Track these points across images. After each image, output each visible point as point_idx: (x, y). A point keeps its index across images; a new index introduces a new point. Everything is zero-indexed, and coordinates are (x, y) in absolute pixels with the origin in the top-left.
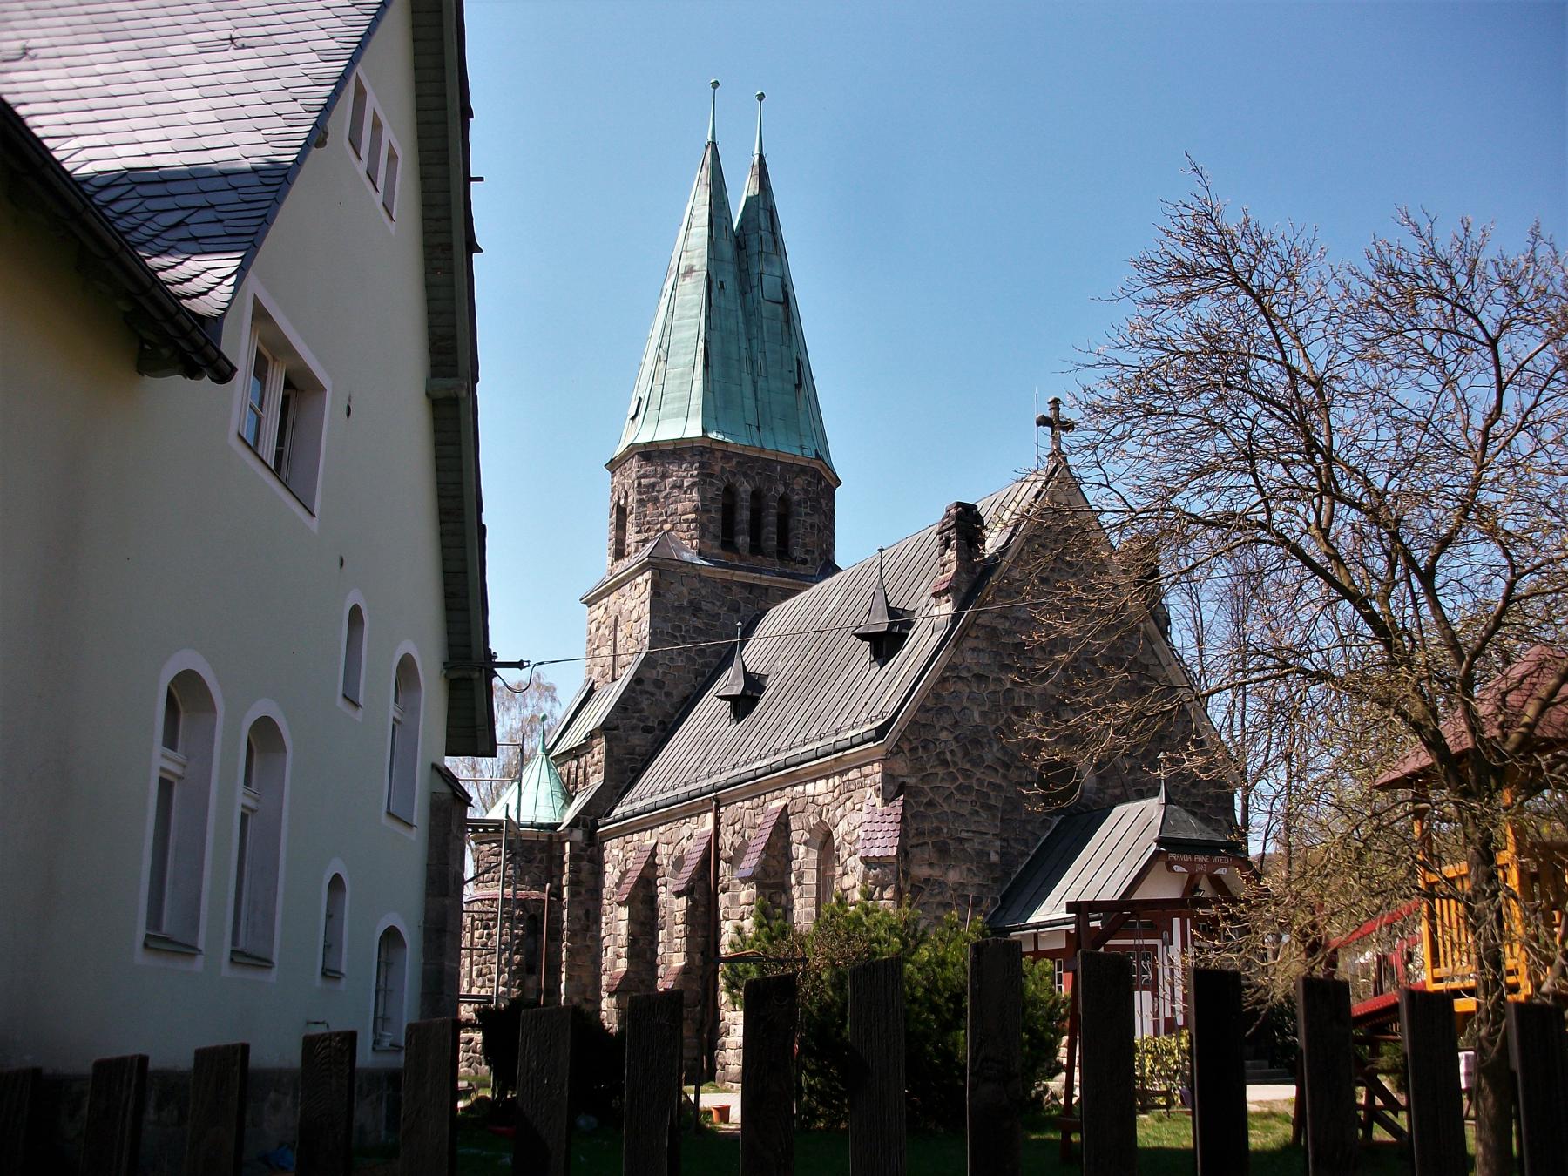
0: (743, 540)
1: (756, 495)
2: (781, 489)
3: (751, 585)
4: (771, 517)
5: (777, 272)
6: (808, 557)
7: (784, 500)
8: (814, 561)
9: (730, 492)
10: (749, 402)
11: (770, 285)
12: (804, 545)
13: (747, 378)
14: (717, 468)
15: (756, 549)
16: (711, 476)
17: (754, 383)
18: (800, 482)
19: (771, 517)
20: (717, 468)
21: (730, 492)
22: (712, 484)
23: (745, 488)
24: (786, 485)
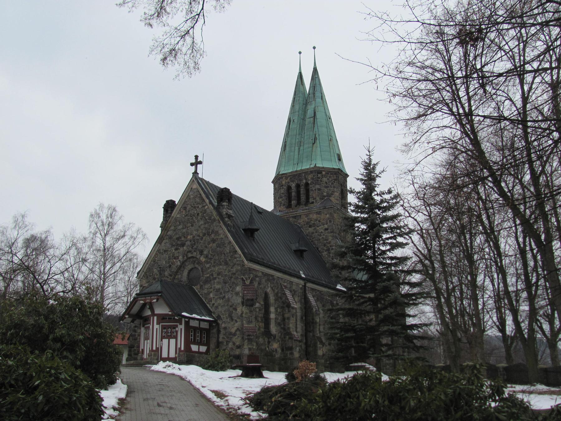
0: (294, 202)
1: (298, 186)
2: (304, 181)
3: (295, 216)
4: (302, 190)
5: (313, 106)
6: (314, 201)
7: (307, 184)
8: (316, 202)
9: (289, 188)
10: (296, 156)
11: (310, 113)
12: (313, 197)
13: (297, 148)
14: (284, 182)
15: (299, 203)
16: (282, 186)
17: (299, 149)
18: (310, 177)
19: (302, 190)
20: (284, 182)
21: (289, 188)
22: (283, 188)
23: (293, 185)
24: (306, 180)
